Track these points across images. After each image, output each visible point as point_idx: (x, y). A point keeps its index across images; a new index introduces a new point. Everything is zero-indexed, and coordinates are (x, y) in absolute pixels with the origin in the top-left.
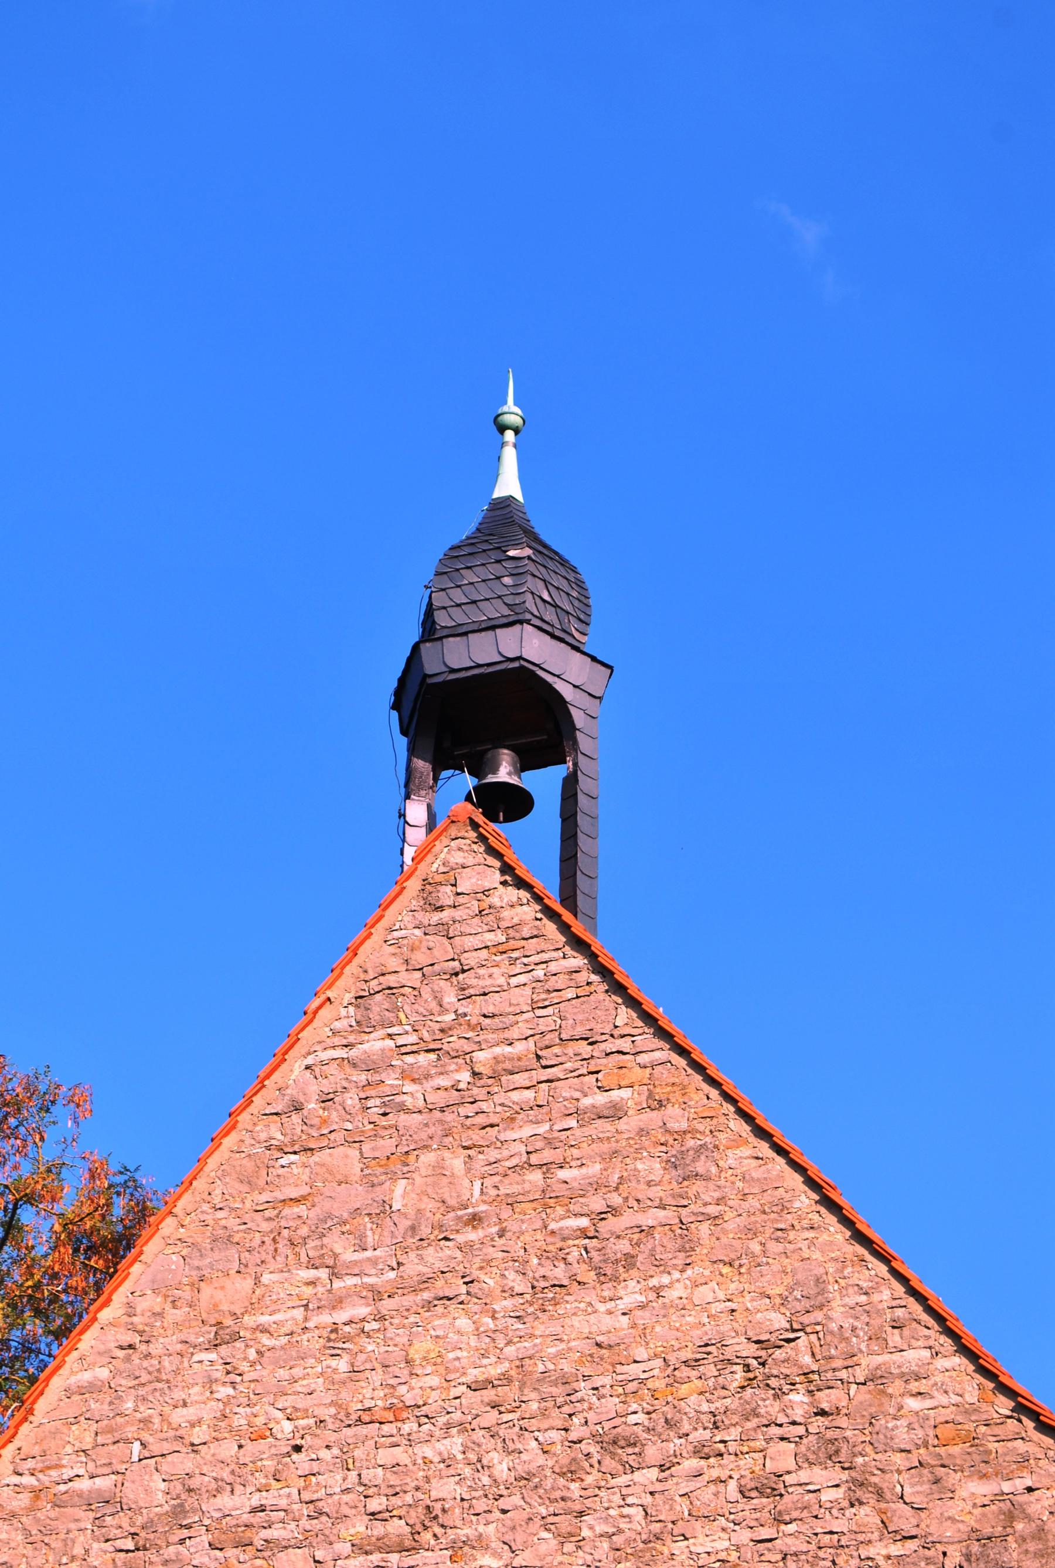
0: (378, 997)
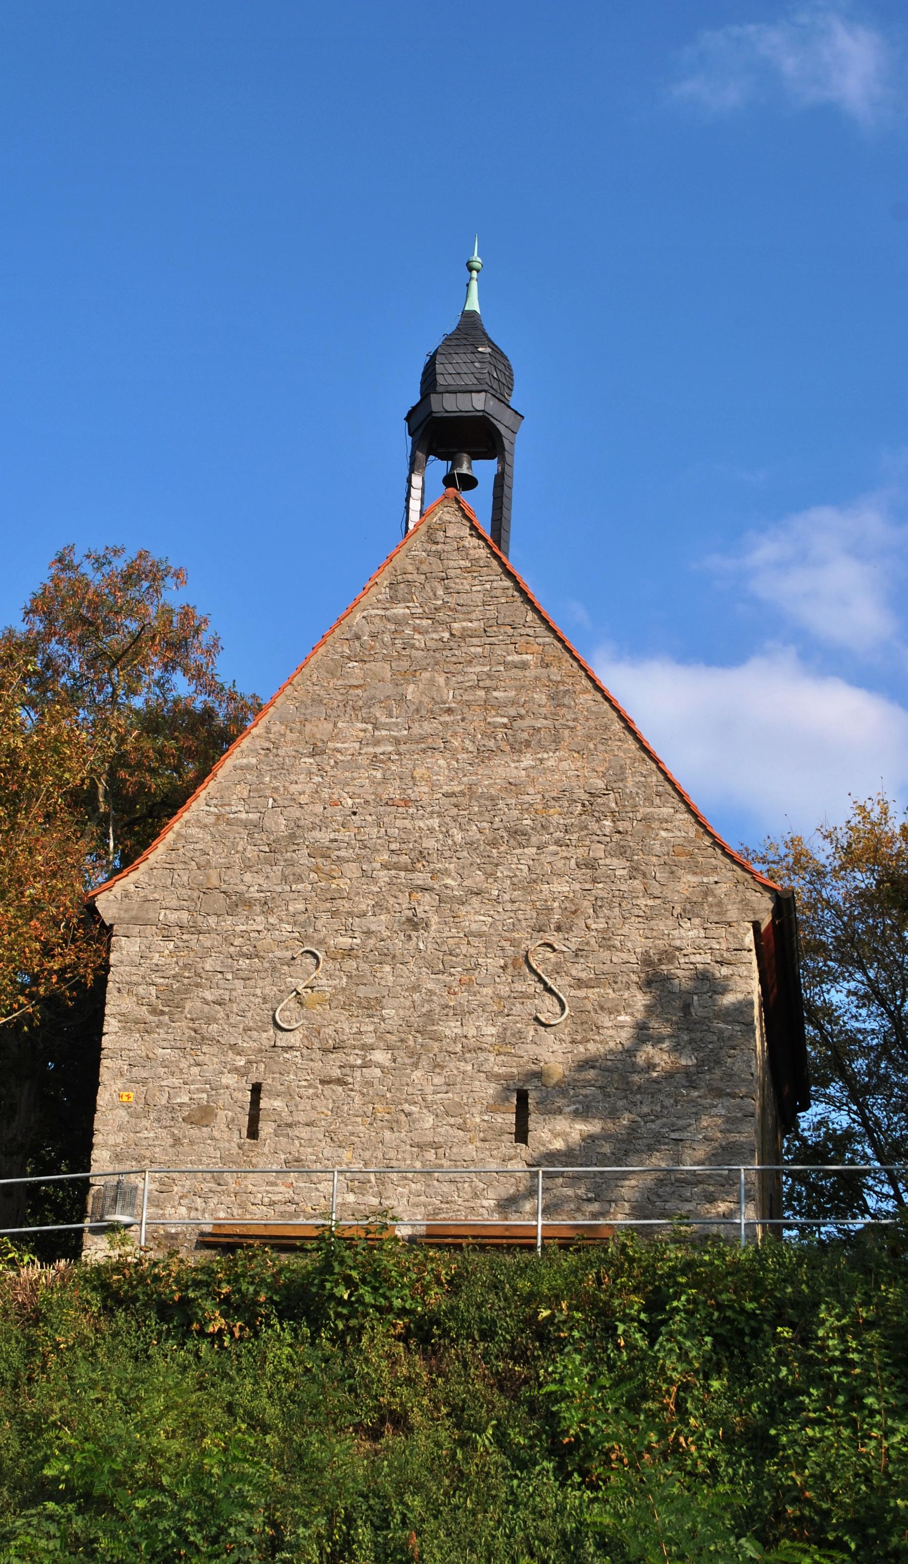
0: (402, 585)
